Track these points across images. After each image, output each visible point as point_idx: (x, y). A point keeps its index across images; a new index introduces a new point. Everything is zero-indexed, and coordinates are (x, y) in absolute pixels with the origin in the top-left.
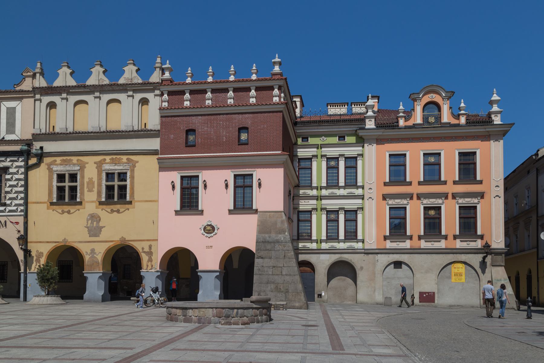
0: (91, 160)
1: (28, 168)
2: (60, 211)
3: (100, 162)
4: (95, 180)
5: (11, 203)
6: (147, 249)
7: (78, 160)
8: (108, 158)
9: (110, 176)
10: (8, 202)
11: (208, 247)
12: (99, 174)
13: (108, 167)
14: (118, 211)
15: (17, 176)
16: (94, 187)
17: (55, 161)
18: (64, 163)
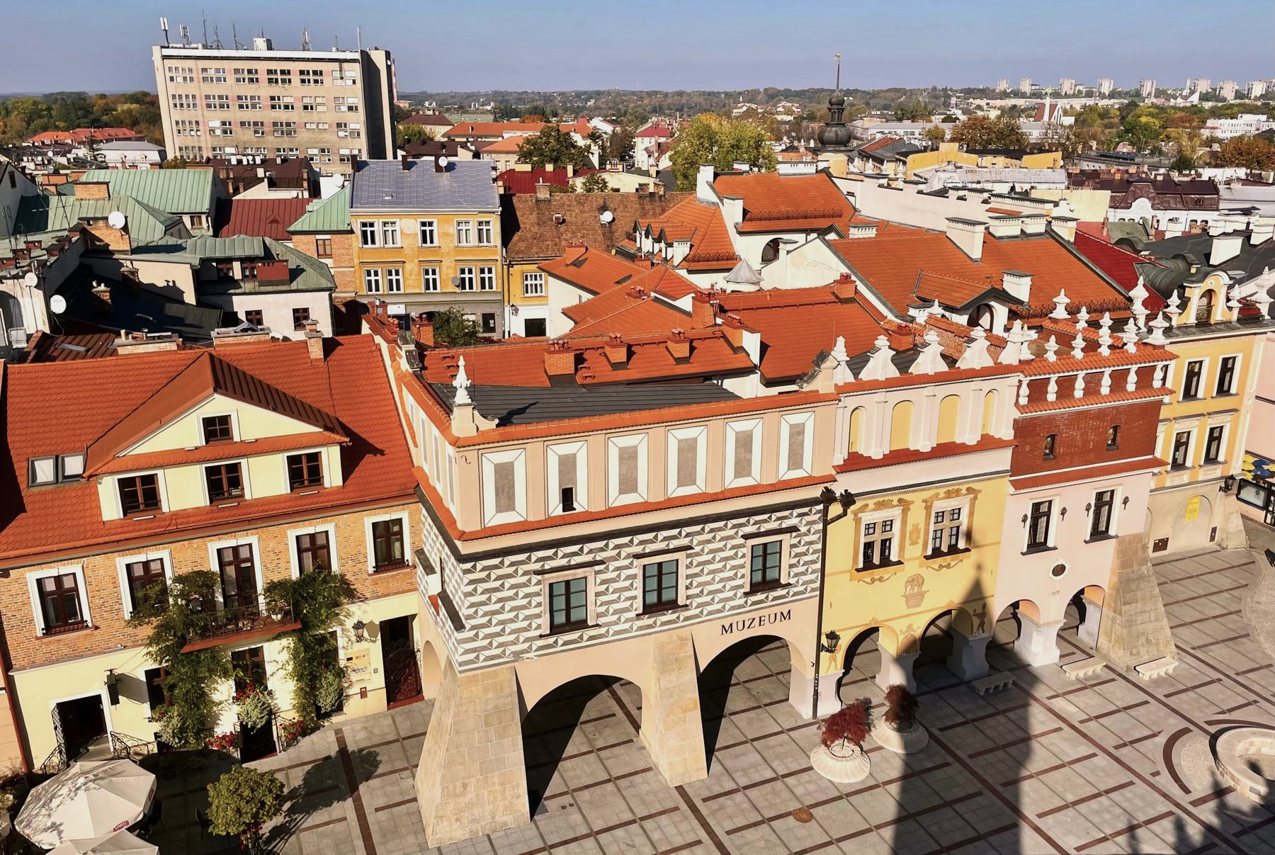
0: (917, 498)
1: (826, 523)
2: (868, 580)
3: (931, 498)
4: (922, 526)
5: (797, 582)
6: (979, 611)
7: (900, 501)
8: (942, 492)
9: (940, 515)
10: (792, 581)
11: (1054, 593)
12: (928, 517)
13: (939, 506)
14: (948, 566)
15: (807, 539)
16: (919, 537)
17: (867, 505)
18: (880, 506)
